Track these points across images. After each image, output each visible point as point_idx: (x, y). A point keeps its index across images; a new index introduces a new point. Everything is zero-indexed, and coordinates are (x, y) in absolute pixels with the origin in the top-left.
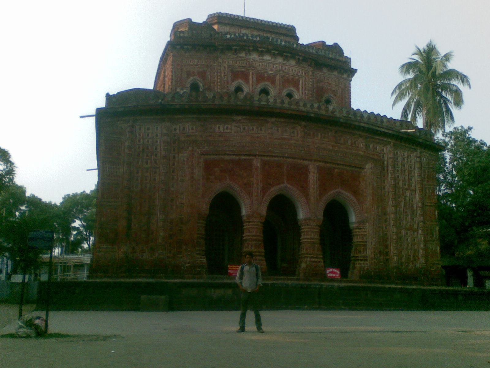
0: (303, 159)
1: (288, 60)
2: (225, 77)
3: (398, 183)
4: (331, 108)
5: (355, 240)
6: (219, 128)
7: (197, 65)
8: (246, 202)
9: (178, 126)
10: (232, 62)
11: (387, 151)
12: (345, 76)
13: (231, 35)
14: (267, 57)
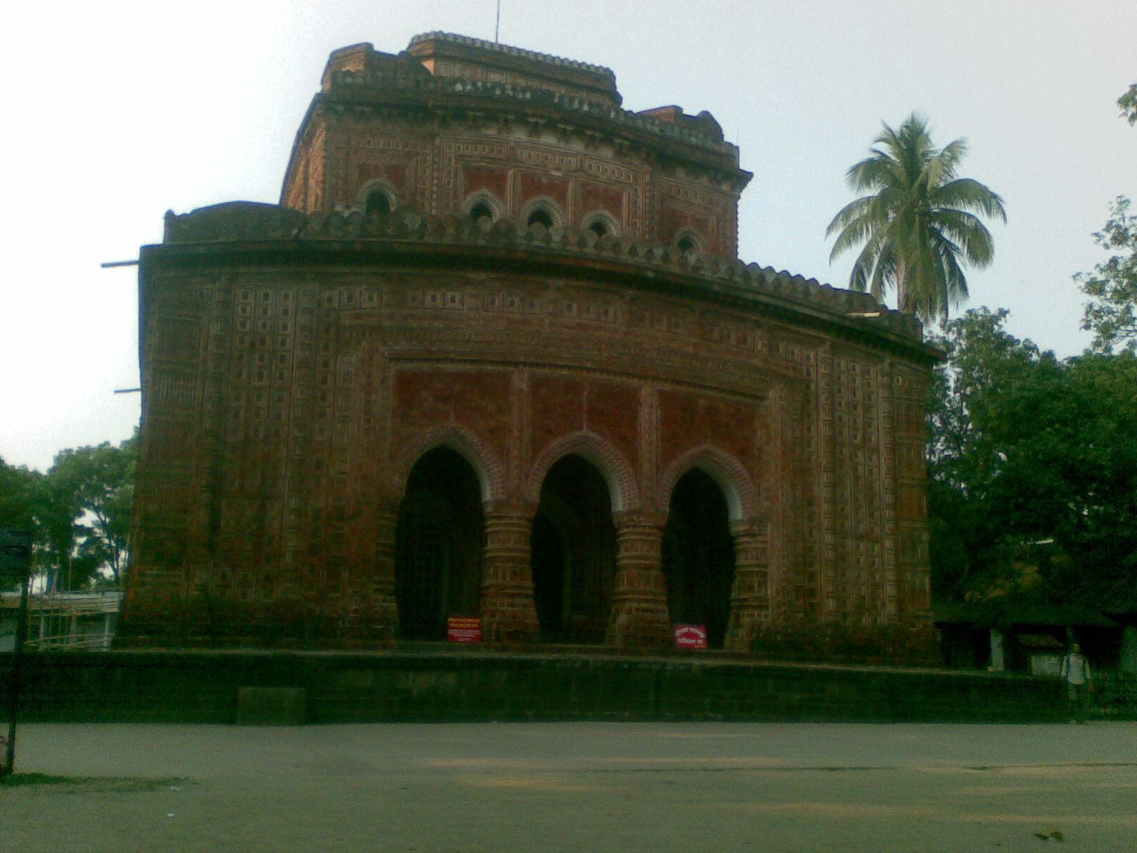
0: (628, 375)
1: (596, 148)
2: (449, 182)
3: (841, 433)
4: (692, 259)
5: (741, 560)
6: (434, 299)
7: (383, 151)
8: (492, 472)
9: (337, 292)
10: (467, 147)
11: (816, 360)
12: (725, 187)
13: (464, 83)
14: (548, 139)
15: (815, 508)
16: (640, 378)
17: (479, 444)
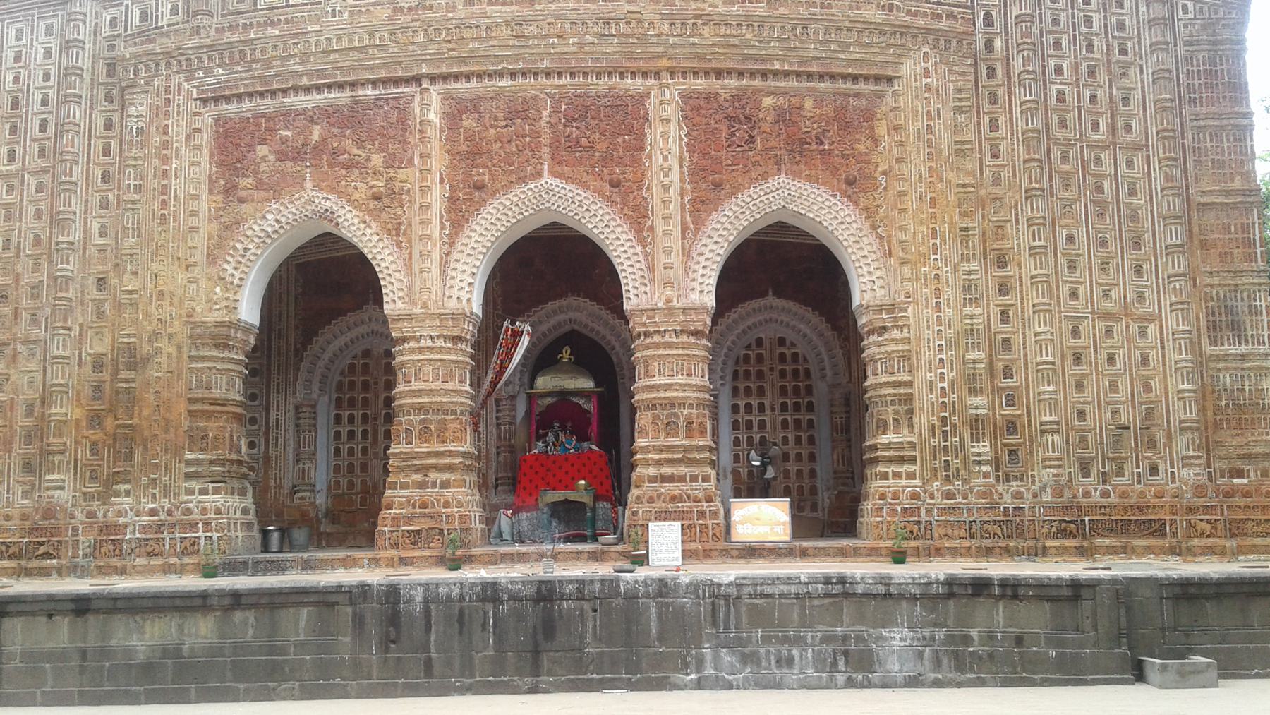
0: (622, 76)
3: (1062, 123)
9: (123, 8)
15: (1011, 270)
16: (645, 74)
17: (356, 221)
